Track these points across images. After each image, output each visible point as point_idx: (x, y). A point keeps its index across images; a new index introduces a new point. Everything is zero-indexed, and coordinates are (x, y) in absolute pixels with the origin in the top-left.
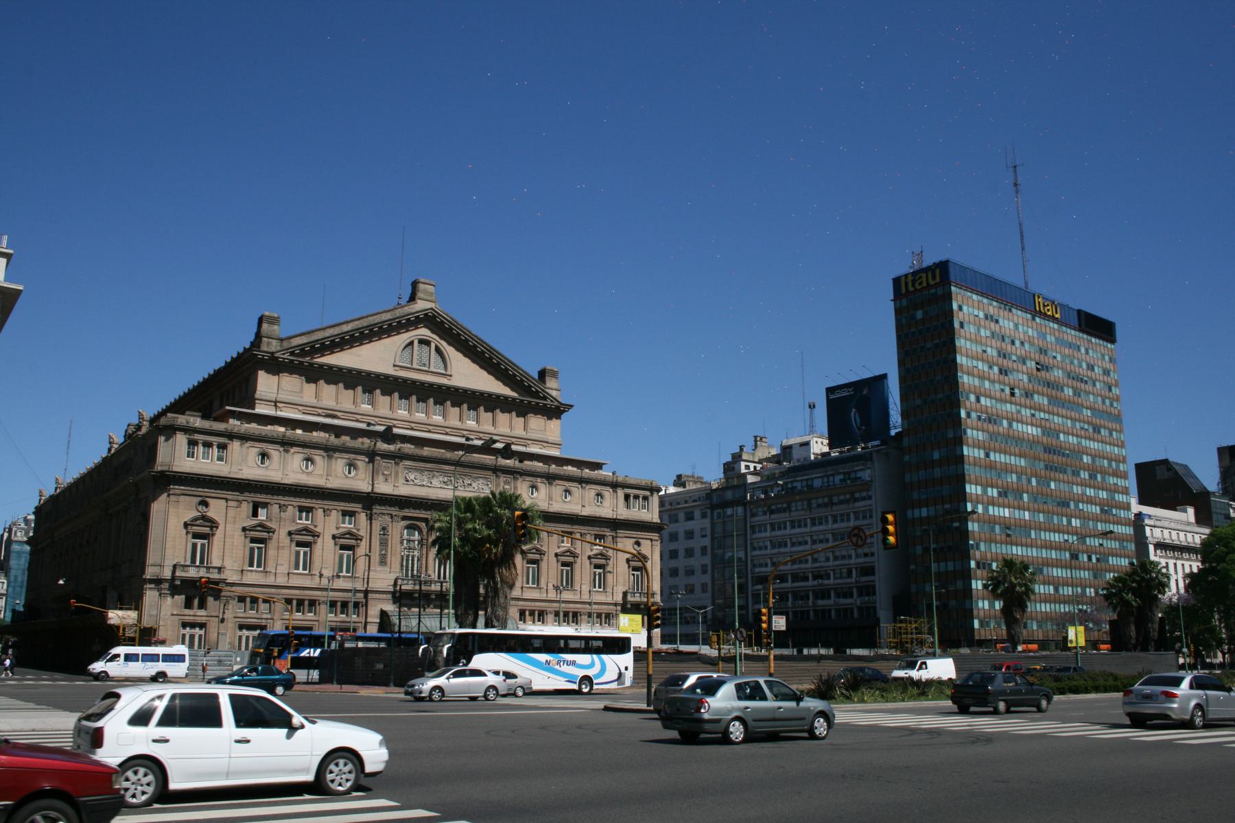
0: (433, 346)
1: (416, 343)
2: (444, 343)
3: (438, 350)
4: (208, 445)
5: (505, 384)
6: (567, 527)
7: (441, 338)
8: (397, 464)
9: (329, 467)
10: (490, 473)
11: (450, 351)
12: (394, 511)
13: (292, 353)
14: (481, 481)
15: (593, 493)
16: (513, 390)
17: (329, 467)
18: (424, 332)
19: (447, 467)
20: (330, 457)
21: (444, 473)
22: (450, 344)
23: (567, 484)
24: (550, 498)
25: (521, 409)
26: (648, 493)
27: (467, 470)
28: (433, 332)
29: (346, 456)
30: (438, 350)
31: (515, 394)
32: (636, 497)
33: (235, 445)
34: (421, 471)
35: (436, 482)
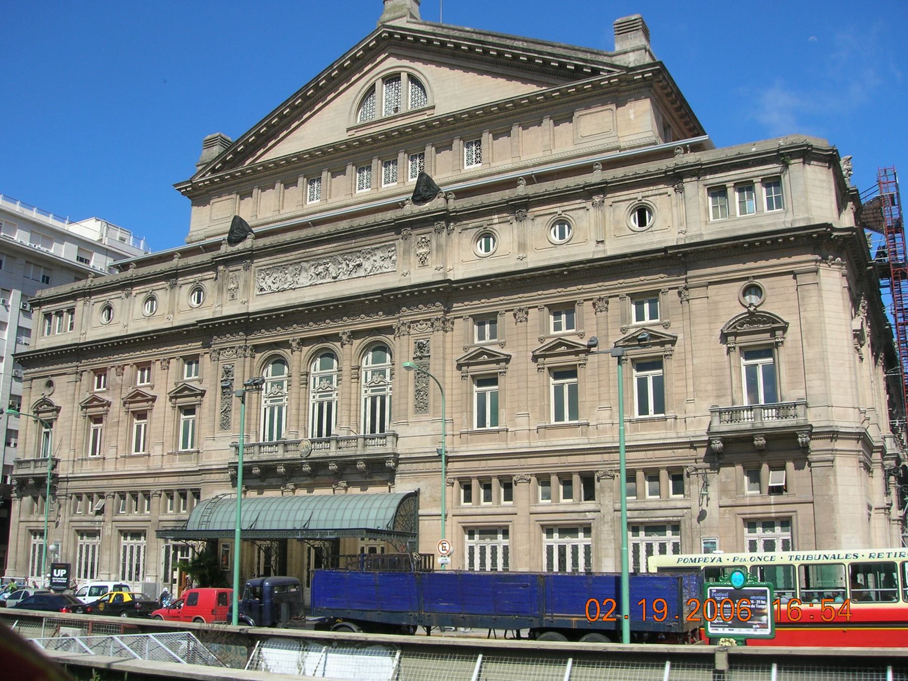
0: (404, 76)
1: (379, 84)
2: (418, 66)
3: (413, 79)
4: (59, 313)
5: (510, 78)
6: (557, 295)
7: (413, 59)
8: (247, 268)
9: (172, 299)
10: (391, 235)
11: (427, 72)
12: (238, 340)
13: (213, 171)
14: (379, 254)
15: (623, 209)
16: (525, 81)
17: (172, 299)
18: (391, 64)
19: (320, 249)
20: (173, 286)
21: (316, 260)
22: (426, 62)
23: (557, 208)
24: (522, 246)
25: (561, 110)
26: (773, 168)
27: (353, 243)
28: (399, 57)
29: (190, 278)
30: (413, 79)
31: (530, 89)
32: (745, 187)
33: (79, 304)
34: (282, 267)
35: (304, 279)
